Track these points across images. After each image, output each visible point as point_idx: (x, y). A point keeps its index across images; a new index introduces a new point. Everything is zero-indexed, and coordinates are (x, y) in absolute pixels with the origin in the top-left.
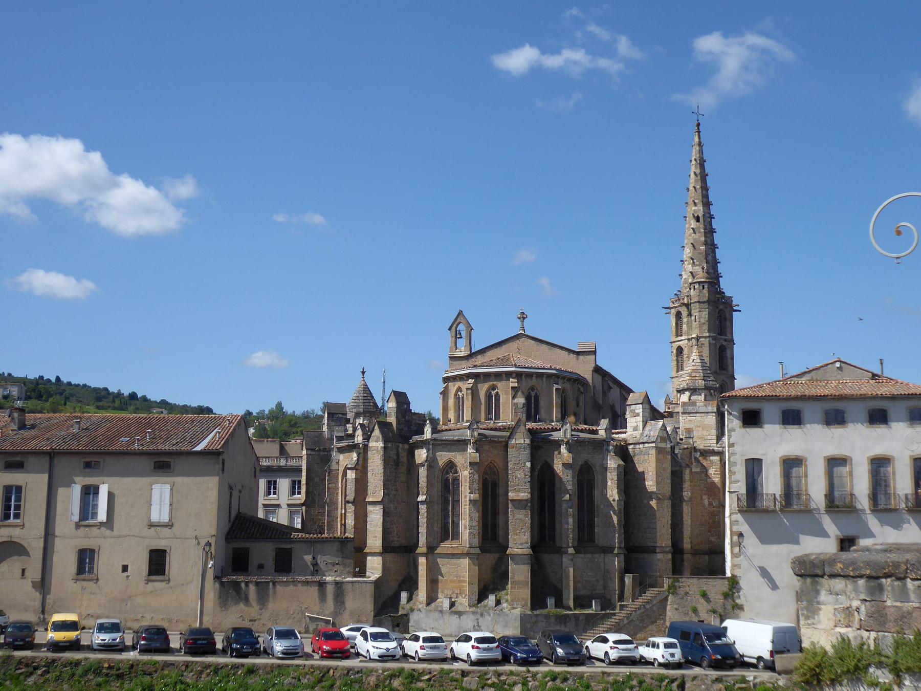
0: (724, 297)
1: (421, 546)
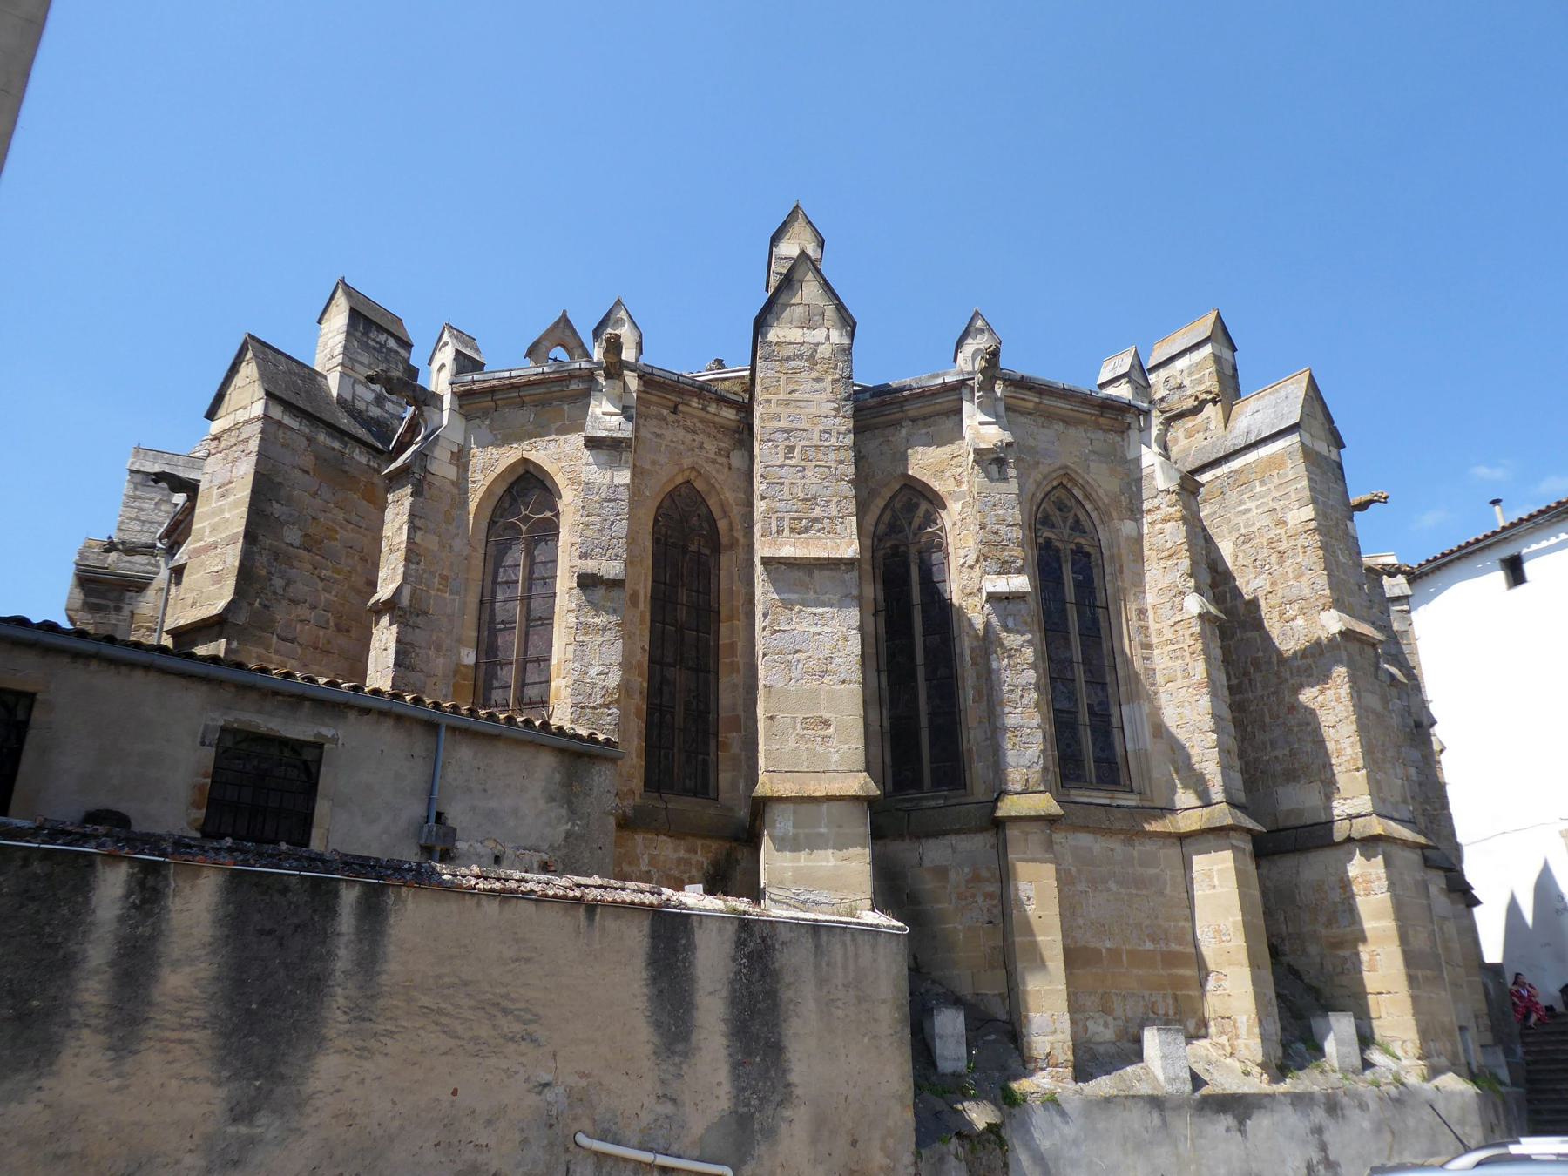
1: (1019, 787)
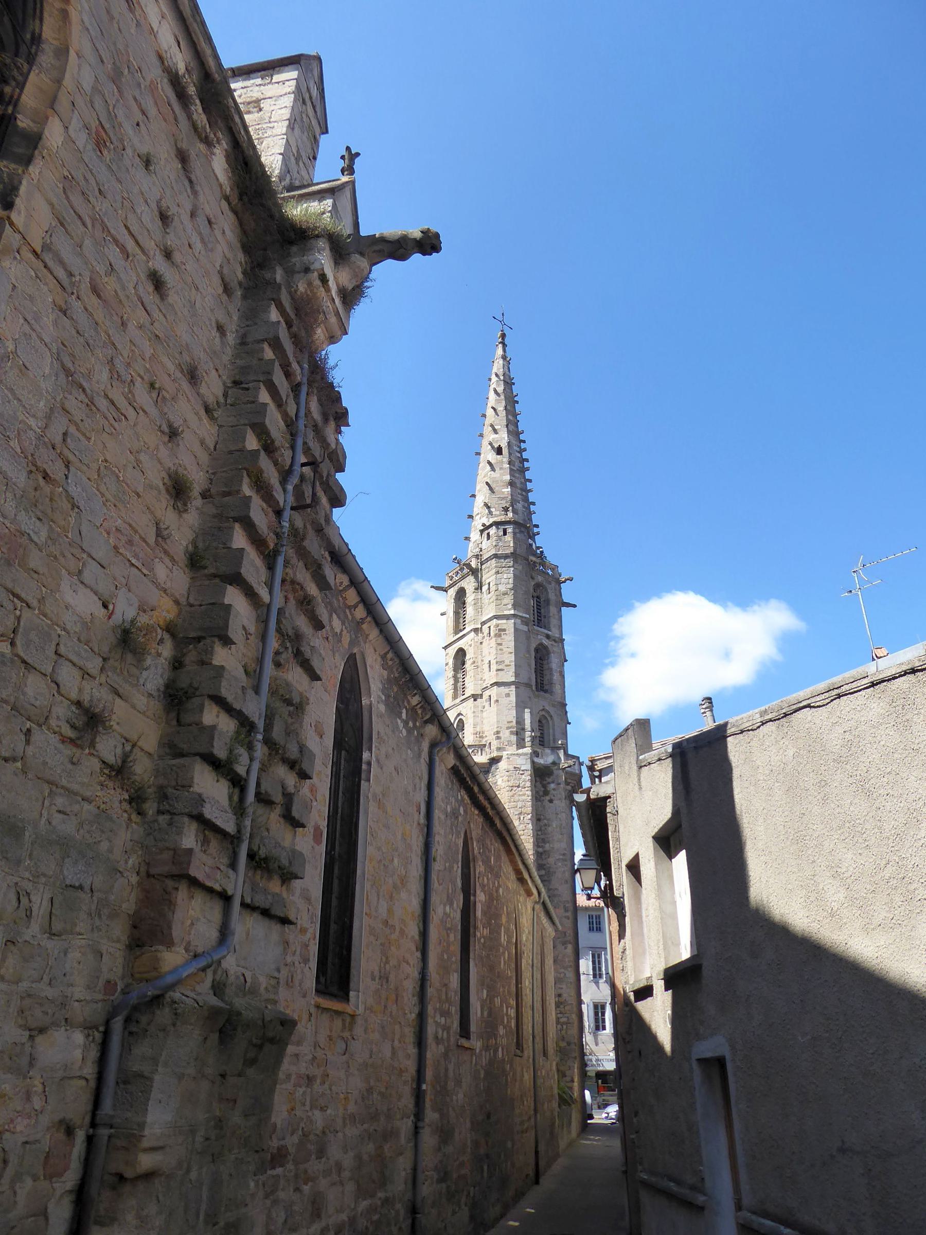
0: (543, 564)
